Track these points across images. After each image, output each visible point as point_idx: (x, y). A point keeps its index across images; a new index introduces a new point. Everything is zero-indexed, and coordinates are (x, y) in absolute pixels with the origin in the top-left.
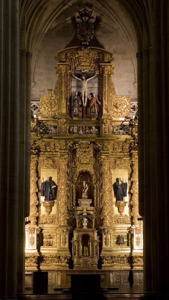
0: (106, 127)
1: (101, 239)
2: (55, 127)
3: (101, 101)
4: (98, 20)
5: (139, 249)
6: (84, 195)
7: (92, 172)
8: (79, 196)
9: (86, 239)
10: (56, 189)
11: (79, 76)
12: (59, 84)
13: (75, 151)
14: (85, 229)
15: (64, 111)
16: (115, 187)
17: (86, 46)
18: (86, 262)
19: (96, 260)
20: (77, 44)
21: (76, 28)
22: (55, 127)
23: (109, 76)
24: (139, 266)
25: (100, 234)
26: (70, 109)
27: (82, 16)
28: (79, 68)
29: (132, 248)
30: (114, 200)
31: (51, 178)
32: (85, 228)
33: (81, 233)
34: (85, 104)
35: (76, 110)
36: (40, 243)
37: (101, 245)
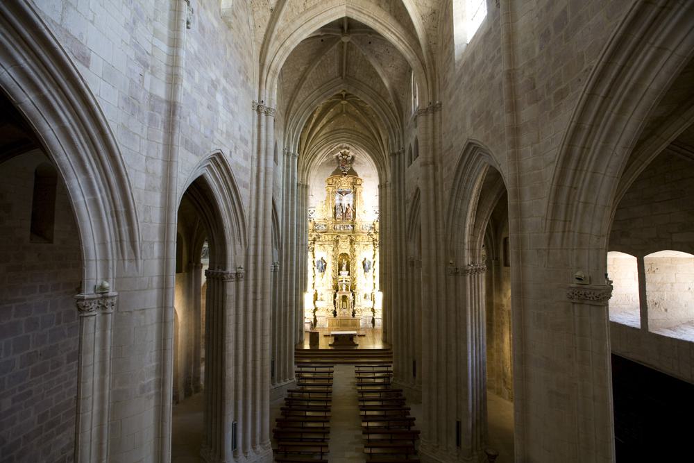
0: (358, 228)
1: (354, 298)
2: (325, 226)
3: (355, 209)
4: (353, 158)
5: (379, 306)
6: (344, 268)
7: (349, 254)
8: (340, 269)
9: (344, 298)
10: (325, 265)
11: (340, 193)
12: (327, 199)
13: (338, 240)
14: (344, 294)
15: (331, 215)
16: (364, 265)
17: (345, 175)
18: (344, 313)
19: (351, 310)
20: (339, 173)
21: (339, 163)
22: (325, 226)
23: (360, 193)
24: (379, 315)
25: (353, 295)
26: (335, 214)
27: (343, 155)
28: (341, 188)
29: (374, 303)
30: (363, 271)
31: (322, 258)
32: (344, 291)
33: (341, 295)
34: (344, 212)
35: (338, 215)
36: (316, 299)
37: (354, 302)
